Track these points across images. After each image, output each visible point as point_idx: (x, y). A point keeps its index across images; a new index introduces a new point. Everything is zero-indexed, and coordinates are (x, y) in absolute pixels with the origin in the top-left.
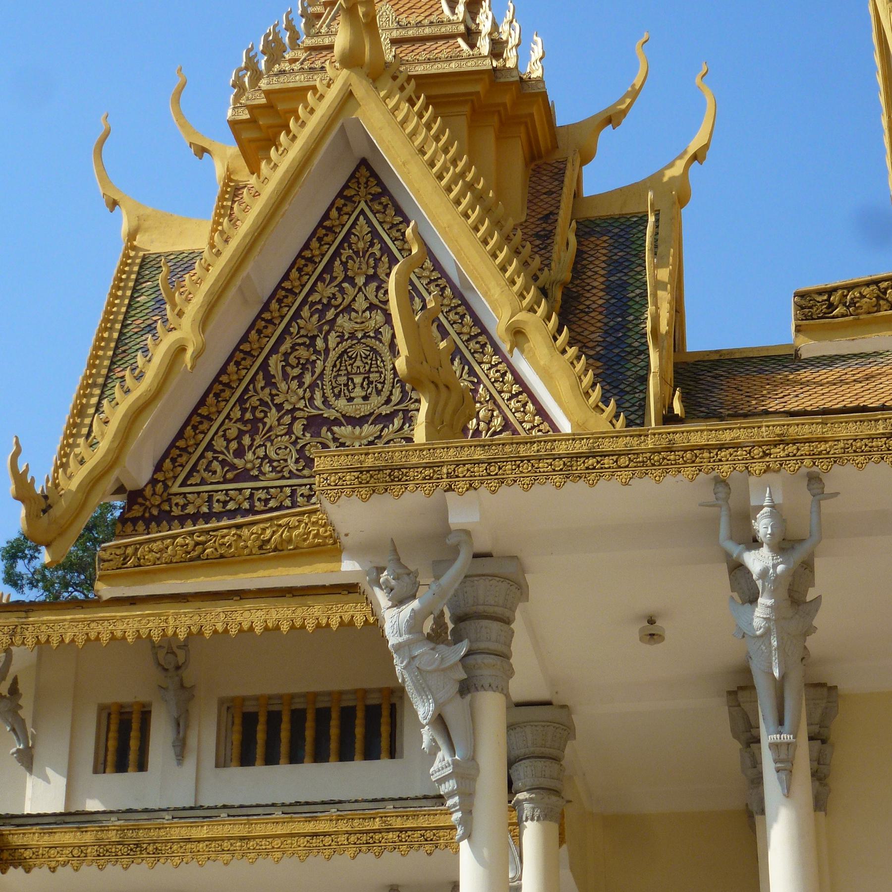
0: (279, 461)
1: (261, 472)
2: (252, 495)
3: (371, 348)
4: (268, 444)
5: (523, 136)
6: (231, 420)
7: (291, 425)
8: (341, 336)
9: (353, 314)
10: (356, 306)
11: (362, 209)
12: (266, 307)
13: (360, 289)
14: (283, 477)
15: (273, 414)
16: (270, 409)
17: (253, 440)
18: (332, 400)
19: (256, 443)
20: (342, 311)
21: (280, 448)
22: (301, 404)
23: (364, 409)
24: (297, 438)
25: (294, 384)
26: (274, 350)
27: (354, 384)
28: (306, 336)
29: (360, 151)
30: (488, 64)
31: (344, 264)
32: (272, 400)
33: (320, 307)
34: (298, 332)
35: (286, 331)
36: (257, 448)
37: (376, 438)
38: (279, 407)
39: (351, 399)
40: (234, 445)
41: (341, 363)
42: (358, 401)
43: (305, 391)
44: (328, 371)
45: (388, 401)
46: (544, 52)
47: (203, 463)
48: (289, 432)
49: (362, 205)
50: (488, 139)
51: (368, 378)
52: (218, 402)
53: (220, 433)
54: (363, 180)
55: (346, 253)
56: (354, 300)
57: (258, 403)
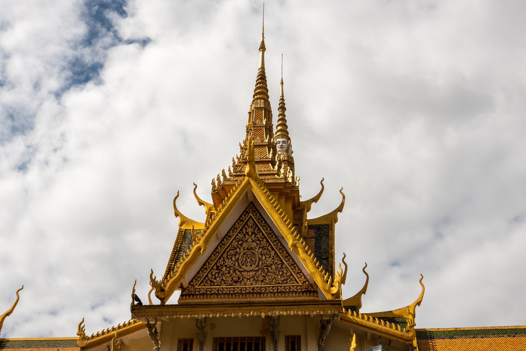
0: (226, 281)
1: (221, 284)
2: (218, 289)
3: (253, 252)
4: (223, 276)
5: (291, 200)
6: (213, 269)
8: (244, 249)
9: (247, 242)
10: (249, 241)
12: (223, 240)
13: (250, 236)
14: (228, 285)
15: (224, 268)
16: (223, 267)
17: (219, 275)
18: (241, 265)
19: (220, 276)
20: (244, 242)
21: (227, 277)
22: (232, 265)
23: (251, 268)
24: (231, 274)
25: (230, 260)
26: (225, 251)
27: (247, 262)
28: (234, 247)
29: (251, 199)
30: (284, 181)
31: (246, 229)
32: (224, 264)
33: (238, 240)
34: (231, 246)
35: (229, 246)
36: (220, 277)
37: (254, 276)
38: (226, 266)
39: (247, 266)
40: (214, 277)
41: (244, 256)
42: (249, 266)
43: (233, 262)
44: (240, 258)
45: (257, 267)
46: (299, 179)
47: (205, 281)
48: (229, 273)
49: (251, 214)
50: (283, 201)
51: (252, 260)
52: (209, 264)
53: (210, 273)
54: (251, 207)
55: (246, 226)
56: (248, 239)
57: (220, 265)
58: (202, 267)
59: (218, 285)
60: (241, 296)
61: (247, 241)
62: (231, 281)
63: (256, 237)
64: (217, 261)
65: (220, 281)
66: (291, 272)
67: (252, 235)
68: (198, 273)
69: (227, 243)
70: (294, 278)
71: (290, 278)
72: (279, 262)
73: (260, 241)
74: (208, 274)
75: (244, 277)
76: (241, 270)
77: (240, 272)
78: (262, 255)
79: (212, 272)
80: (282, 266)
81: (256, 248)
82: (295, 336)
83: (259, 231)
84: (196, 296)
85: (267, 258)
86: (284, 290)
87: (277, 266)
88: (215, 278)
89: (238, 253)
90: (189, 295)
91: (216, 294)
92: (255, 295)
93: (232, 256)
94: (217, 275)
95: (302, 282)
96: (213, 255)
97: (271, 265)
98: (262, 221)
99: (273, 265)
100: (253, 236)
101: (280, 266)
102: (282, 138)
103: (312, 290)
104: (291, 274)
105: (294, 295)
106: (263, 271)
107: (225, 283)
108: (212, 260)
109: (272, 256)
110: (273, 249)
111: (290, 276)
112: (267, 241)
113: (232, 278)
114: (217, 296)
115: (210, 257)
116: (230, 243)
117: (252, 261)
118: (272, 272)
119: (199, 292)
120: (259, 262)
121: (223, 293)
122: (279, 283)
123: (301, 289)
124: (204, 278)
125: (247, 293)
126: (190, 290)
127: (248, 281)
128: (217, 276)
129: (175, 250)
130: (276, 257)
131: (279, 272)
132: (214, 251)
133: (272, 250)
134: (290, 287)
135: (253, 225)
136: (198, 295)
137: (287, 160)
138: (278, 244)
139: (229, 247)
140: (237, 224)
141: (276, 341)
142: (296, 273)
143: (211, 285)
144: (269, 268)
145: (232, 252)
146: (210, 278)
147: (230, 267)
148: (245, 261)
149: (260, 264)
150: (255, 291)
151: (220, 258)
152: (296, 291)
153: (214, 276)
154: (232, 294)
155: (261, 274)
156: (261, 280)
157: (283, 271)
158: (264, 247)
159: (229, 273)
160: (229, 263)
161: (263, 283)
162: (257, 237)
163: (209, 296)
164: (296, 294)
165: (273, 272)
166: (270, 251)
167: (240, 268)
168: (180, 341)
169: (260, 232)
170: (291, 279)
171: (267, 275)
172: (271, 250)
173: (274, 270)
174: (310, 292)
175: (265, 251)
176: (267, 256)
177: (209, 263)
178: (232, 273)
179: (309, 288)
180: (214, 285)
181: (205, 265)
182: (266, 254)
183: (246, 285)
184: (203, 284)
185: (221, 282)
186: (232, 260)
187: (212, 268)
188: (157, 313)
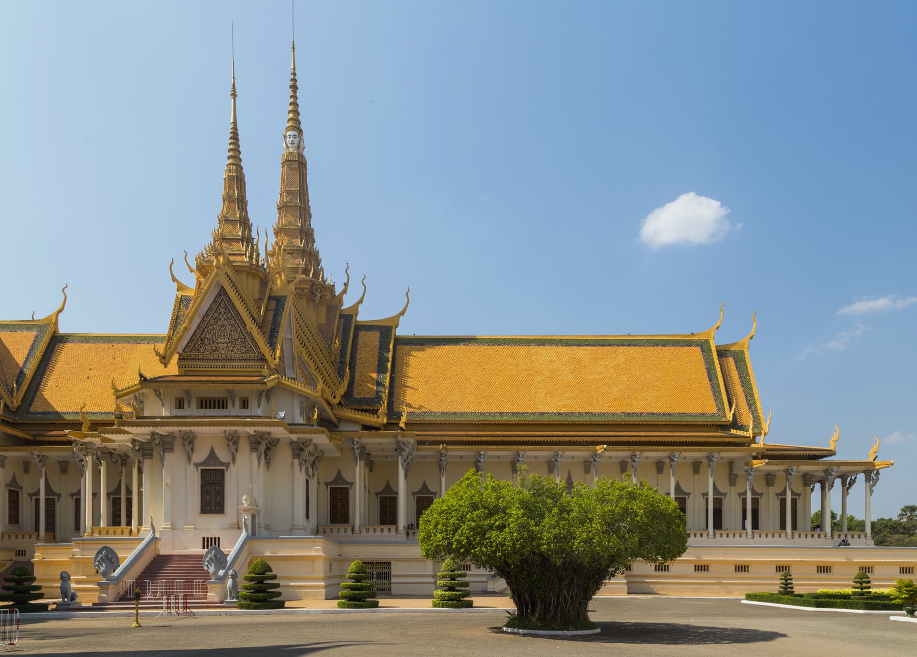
5: (258, 279)
12: (204, 318)
15: (206, 340)
23: (224, 341)
26: (205, 327)
35: (208, 323)
38: (207, 338)
47: (194, 349)
61: (220, 319)
67: (224, 314)
68: (189, 343)
72: (243, 337)
77: (217, 343)
78: (231, 331)
80: (245, 340)
88: (201, 347)
90: (184, 359)
92: (227, 361)
94: (201, 345)
97: (238, 339)
100: (225, 315)
101: (243, 340)
104: (251, 347)
106: (232, 343)
110: (239, 327)
112: (235, 320)
115: (196, 331)
122: (243, 353)
124: (193, 347)
132: (198, 326)
143: (198, 353)
145: (210, 327)
149: (230, 338)
151: (203, 332)
154: (212, 360)
159: (210, 344)
160: (209, 336)
168: (176, 398)
174: (261, 360)
175: (234, 328)
180: (200, 352)
181: (192, 337)
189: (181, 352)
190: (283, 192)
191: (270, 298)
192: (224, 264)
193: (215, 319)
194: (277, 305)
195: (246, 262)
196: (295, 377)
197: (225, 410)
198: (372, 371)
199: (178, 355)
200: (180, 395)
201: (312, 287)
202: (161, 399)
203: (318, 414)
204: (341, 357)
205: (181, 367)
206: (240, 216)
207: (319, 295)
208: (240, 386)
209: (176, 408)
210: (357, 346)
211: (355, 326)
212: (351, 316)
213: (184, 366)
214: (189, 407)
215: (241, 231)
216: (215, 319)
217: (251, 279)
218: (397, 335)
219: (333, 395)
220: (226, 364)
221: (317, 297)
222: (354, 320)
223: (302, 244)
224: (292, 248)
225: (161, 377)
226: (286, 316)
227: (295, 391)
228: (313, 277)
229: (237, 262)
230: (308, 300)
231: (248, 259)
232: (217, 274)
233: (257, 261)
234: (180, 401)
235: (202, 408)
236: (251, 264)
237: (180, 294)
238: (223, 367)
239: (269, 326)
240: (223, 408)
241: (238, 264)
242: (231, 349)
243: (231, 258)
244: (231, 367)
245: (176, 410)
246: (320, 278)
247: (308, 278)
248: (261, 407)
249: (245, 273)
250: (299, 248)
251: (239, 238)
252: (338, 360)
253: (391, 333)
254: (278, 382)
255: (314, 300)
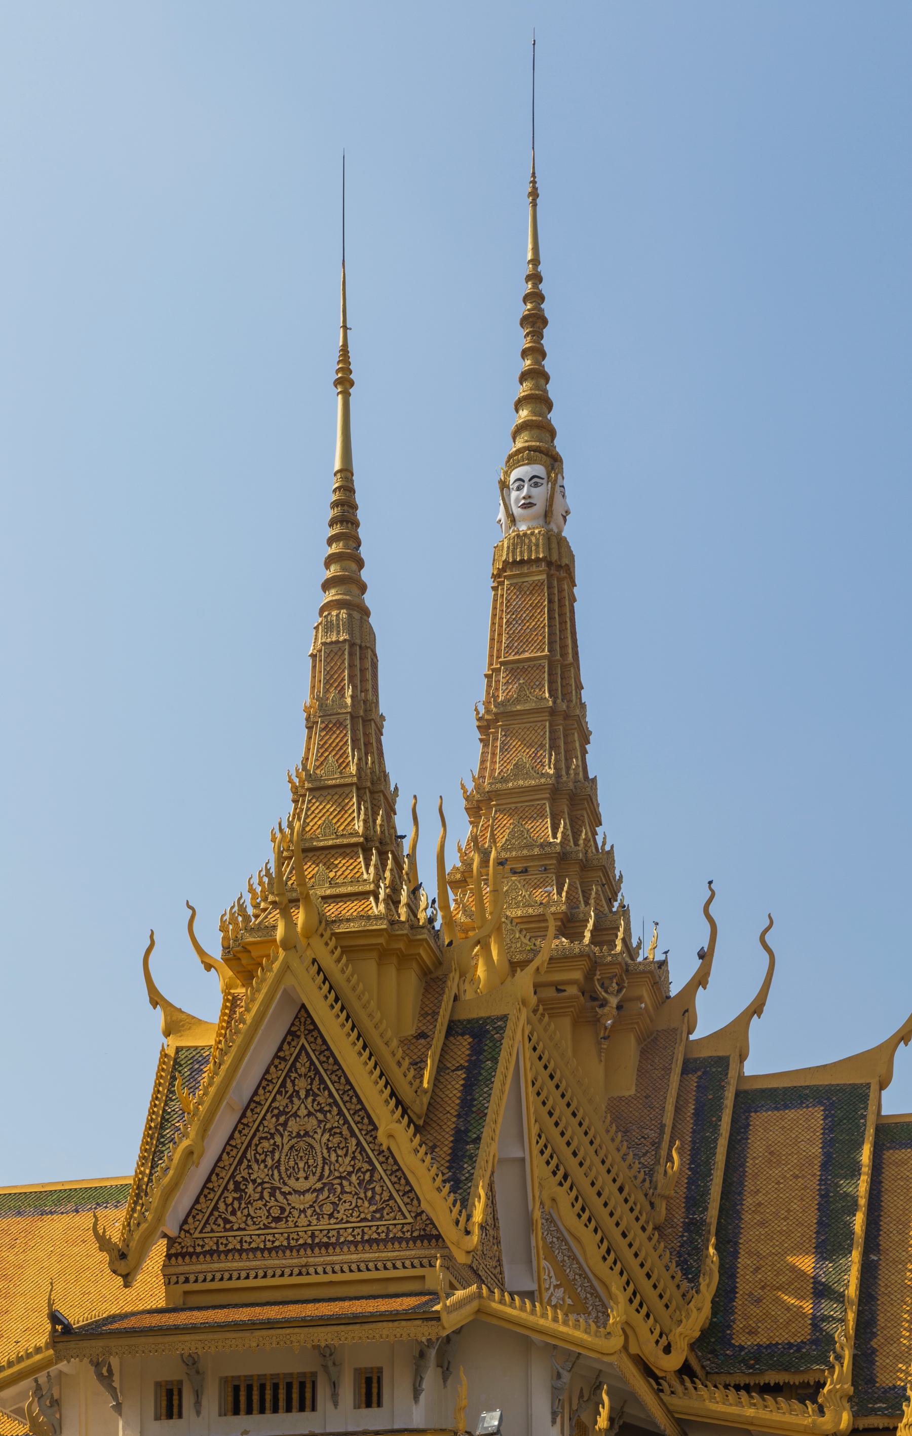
1: (247, 1225)
4: (249, 1206)
5: (415, 965)
6: (228, 1190)
7: (262, 1193)
9: (298, 1119)
11: (303, 1045)
12: (243, 1115)
13: (303, 1102)
14: (260, 1229)
15: (251, 1186)
17: (240, 1204)
18: (286, 1179)
19: (243, 1206)
20: (291, 1116)
21: (256, 1209)
22: (267, 1180)
24: (267, 1201)
25: (262, 1166)
32: (250, 1177)
35: (257, 1130)
40: (230, 1209)
45: (321, 1178)
48: (261, 1198)
51: (307, 1163)
53: (222, 1200)
56: (298, 1109)
57: (241, 1179)
58: (204, 1187)
59: (239, 1229)
60: (288, 1253)
61: (295, 1115)
62: (267, 1217)
63: (316, 1103)
64: (235, 1169)
65: (244, 1218)
66: (390, 1192)
67: (306, 1097)
68: (197, 1201)
69: (254, 1121)
70: (396, 1206)
71: (388, 1205)
72: (366, 1166)
73: (324, 1113)
74: (217, 1203)
75: (294, 1208)
76: (286, 1189)
77: (284, 1194)
78: (329, 1149)
79: (225, 1198)
81: (316, 1132)
82: (372, 1368)
83: (322, 1086)
84: (198, 1258)
85: (341, 1156)
86: (375, 1236)
87: (362, 1178)
88: (233, 1213)
89: (278, 1146)
90: (183, 1256)
91: (238, 1250)
92: (317, 1250)
93: (266, 1156)
94: (236, 1204)
95: (413, 1215)
96: (225, 1154)
97: (350, 1174)
98: (328, 1058)
99: (353, 1175)
100: (310, 1099)
101: (368, 1174)
102: (531, 461)
103: (435, 1232)
104: (391, 1197)
105: (396, 1245)
106: (332, 1190)
107: (254, 1223)
108: (223, 1168)
109: (350, 1152)
111: (388, 1200)
112: (340, 1113)
113: (268, 1211)
114: (241, 1255)
115: (220, 1159)
116: (261, 1123)
117: (309, 1167)
118: (350, 1193)
119: (203, 1246)
120: (323, 1167)
121: (252, 1248)
122: (365, 1220)
123: (412, 1232)
124: (211, 1214)
125: (300, 1245)
126: (183, 1244)
127: (303, 1215)
128: (238, 1205)
129: (153, 1125)
130: (360, 1153)
131: (366, 1190)
132: (228, 1143)
133: (351, 1136)
134: (388, 1228)
135: (309, 1071)
136: (201, 1253)
137: (545, 558)
138: (363, 1118)
139: (259, 1131)
140: (273, 1069)
141: (334, 1383)
142: (401, 1194)
143: (226, 1230)
144: (345, 1183)
145: (265, 1144)
146: (223, 1213)
147: (263, 1182)
148: (293, 1167)
149: (326, 1173)
150: (317, 1240)
151: (240, 1162)
152: (401, 1237)
153: (230, 1207)
154: (270, 1250)
155: (328, 1197)
156: (329, 1213)
157: (373, 1189)
158: (333, 1128)
159: (261, 1198)
160: (259, 1173)
161: (333, 1221)
162: (319, 1104)
163: (223, 1256)
164: (400, 1243)
165: (353, 1193)
166: (346, 1139)
167: (285, 1184)
168: (158, 1385)
169: (324, 1090)
170: (391, 1208)
171: (340, 1199)
172: (349, 1135)
173: (355, 1187)
175: (337, 1139)
176: (340, 1152)
177: (217, 1175)
178: (268, 1199)
179: (428, 1229)
180: (231, 1229)
181: (209, 1180)
182: (339, 1147)
183: (298, 1226)
184: (208, 1229)
185: (245, 1222)
186: (266, 1166)
187: (226, 1188)
188: (101, 1349)
189: (173, 1232)
190: (497, 671)
191: (453, 1029)
192: (308, 933)
193: (277, 1117)
194: (477, 1050)
195: (377, 918)
196: (534, 1287)
197: (307, 1414)
198: (798, 1249)
199: (164, 1241)
200: (173, 1372)
201: (589, 976)
202: (113, 1391)
203: (612, 1409)
204: (688, 1209)
205: (174, 1279)
206: (359, 769)
207: (614, 1001)
208: (356, 1330)
209: (157, 1418)
210: (743, 1165)
211: (738, 1094)
212: (723, 1063)
213: (182, 1279)
214: (198, 1413)
215: (362, 817)
216: (277, 1117)
217: (391, 972)
218: (884, 1112)
219: (663, 1342)
220: (312, 1259)
221: (606, 1010)
222: (732, 1073)
223: (559, 835)
224: (525, 852)
225: (113, 1318)
226: (504, 1084)
227: (534, 1336)
228: (592, 942)
229: (348, 920)
230: (576, 1023)
231: (382, 907)
232: (286, 968)
233: (413, 909)
234: (170, 1393)
235: (236, 1412)
236: (392, 923)
237: (173, 1043)
238: (304, 1270)
239: (450, 1123)
240: (302, 1409)
241: (353, 927)
242: (328, 1209)
243: (331, 910)
244: (329, 1269)
245: (158, 1422)
246: (619, 942)
247: (576, 948)
248: (422, 1397)
249: (375, 954)
250: (547, 849)
251: (354, 840)
252: (679, 1217)
253: (866, 1108)
254: (479, 1311)
255: (596, 1021)
